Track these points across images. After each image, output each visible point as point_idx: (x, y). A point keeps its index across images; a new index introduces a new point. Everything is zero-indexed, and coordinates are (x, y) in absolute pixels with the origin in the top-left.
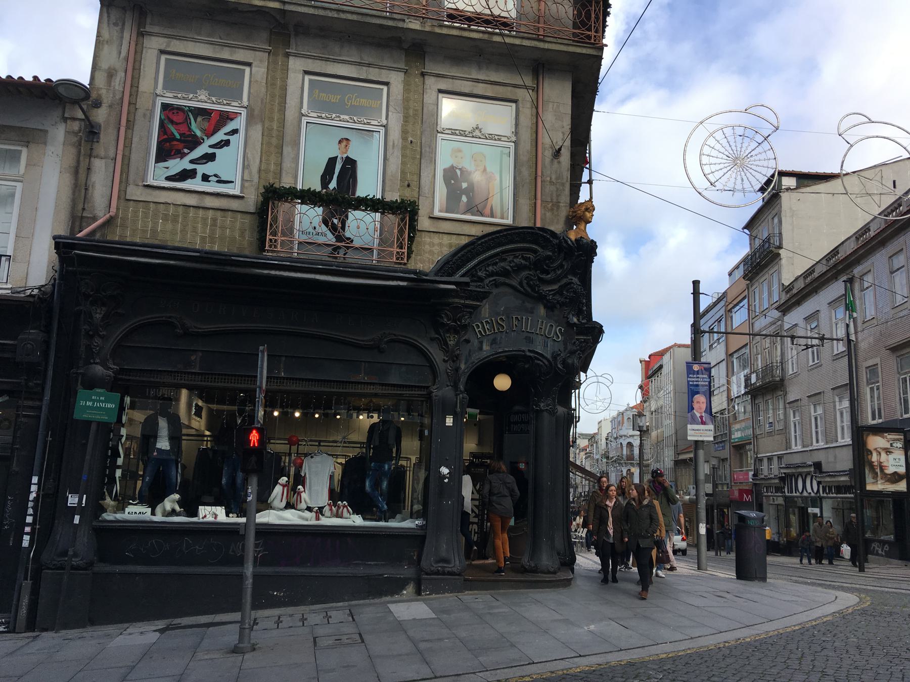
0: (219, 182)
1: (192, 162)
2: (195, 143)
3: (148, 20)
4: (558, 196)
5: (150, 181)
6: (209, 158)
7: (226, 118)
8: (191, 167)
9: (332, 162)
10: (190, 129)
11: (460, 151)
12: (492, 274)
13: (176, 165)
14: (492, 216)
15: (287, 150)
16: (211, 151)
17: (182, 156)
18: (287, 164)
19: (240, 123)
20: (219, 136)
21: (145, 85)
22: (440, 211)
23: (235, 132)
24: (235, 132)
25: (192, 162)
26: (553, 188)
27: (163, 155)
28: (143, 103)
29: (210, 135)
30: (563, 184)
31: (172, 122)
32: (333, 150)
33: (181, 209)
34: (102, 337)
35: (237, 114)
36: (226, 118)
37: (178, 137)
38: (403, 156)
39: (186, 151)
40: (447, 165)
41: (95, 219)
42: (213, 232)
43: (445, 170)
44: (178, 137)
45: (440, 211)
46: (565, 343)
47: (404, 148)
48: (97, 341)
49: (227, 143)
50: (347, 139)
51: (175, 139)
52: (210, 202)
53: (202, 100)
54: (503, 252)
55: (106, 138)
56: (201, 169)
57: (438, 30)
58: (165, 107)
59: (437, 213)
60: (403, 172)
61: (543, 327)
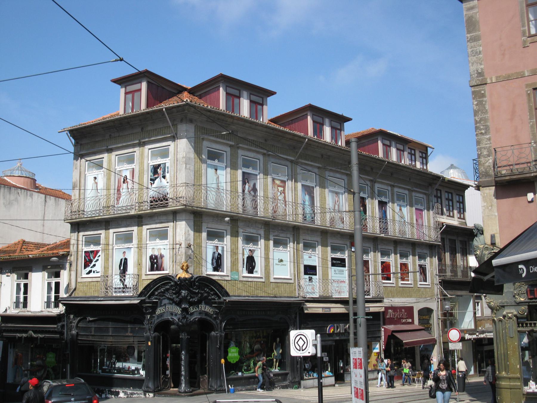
0: (97, 272)
1: (91, 267)
2: (91, 261)
3: (80, 227)
4: (181, 260)
5: (83, 276)
6: (94, 265)
7: (97, 252)
8: (90, 269)
9: (121, 260)
10: (90, 258)
11: (154, 249)
12: (159, 293)
13: (88, 269)
14: (163, 270)
15: (110, 260)
16: (95, 263)
17: (89, 266)
18: (110, 264)
19: (100, 254)
20: (96, 258)
21: (80, 246)
22: (149, 271)
23: (99, 256)
24: (99, 256)
25: (91, 267)
26: (180, 257)
27: (86, 266)
28: (80, 253)
29: (94, 258)
30: (183, 255)
31: (87, 256)
32: (122, 257)
33: (89, 283)
34: (74, 323)
35: (100, 250)
36: (97, 252)
37: (88, 260)
38: (138, 254)
39: (90, 264)
40: (150, 255)
41: (72, 289)
42: (95, 288)
43: (150, 257)
44: (88, 260)
45: (149, 271)
46: (182, 314)
47: (138, 252)
48: (73, 324)
49: (98, 260)
50: (125, 252)
51: (87, 261)
52: (95, 280)
53: (92, 248)
54: (162, 285)
55: (74, 265)
56: (93, 269)
57: (139, 213)
58: (85, 252)
59: (148, 273)
60: (138, 260)
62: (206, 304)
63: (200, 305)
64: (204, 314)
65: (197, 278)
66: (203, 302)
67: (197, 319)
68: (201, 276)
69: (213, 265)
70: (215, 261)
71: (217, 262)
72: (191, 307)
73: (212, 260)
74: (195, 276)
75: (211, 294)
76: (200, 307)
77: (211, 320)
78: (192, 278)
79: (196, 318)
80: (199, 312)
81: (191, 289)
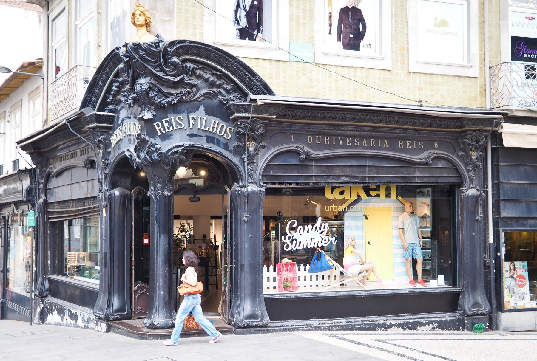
61: (132, 129)
62: (209, 112)
63: (190, 117)
64: (205, 138)
65: (172, 43)
66: (202, 108)
67: (180, 149)
68: (184, 41)
69: (238, 24)
70: (243, 13)
71: (250, 15)
72: (163, 121)
73: (236, 11)
74: (168, 38)
75: (225, 90)
76: (191, 122)
77: (226, 153)
78: (157, 45)
79: (178, 146)
80: (188, 132)
81: (161, 74)
